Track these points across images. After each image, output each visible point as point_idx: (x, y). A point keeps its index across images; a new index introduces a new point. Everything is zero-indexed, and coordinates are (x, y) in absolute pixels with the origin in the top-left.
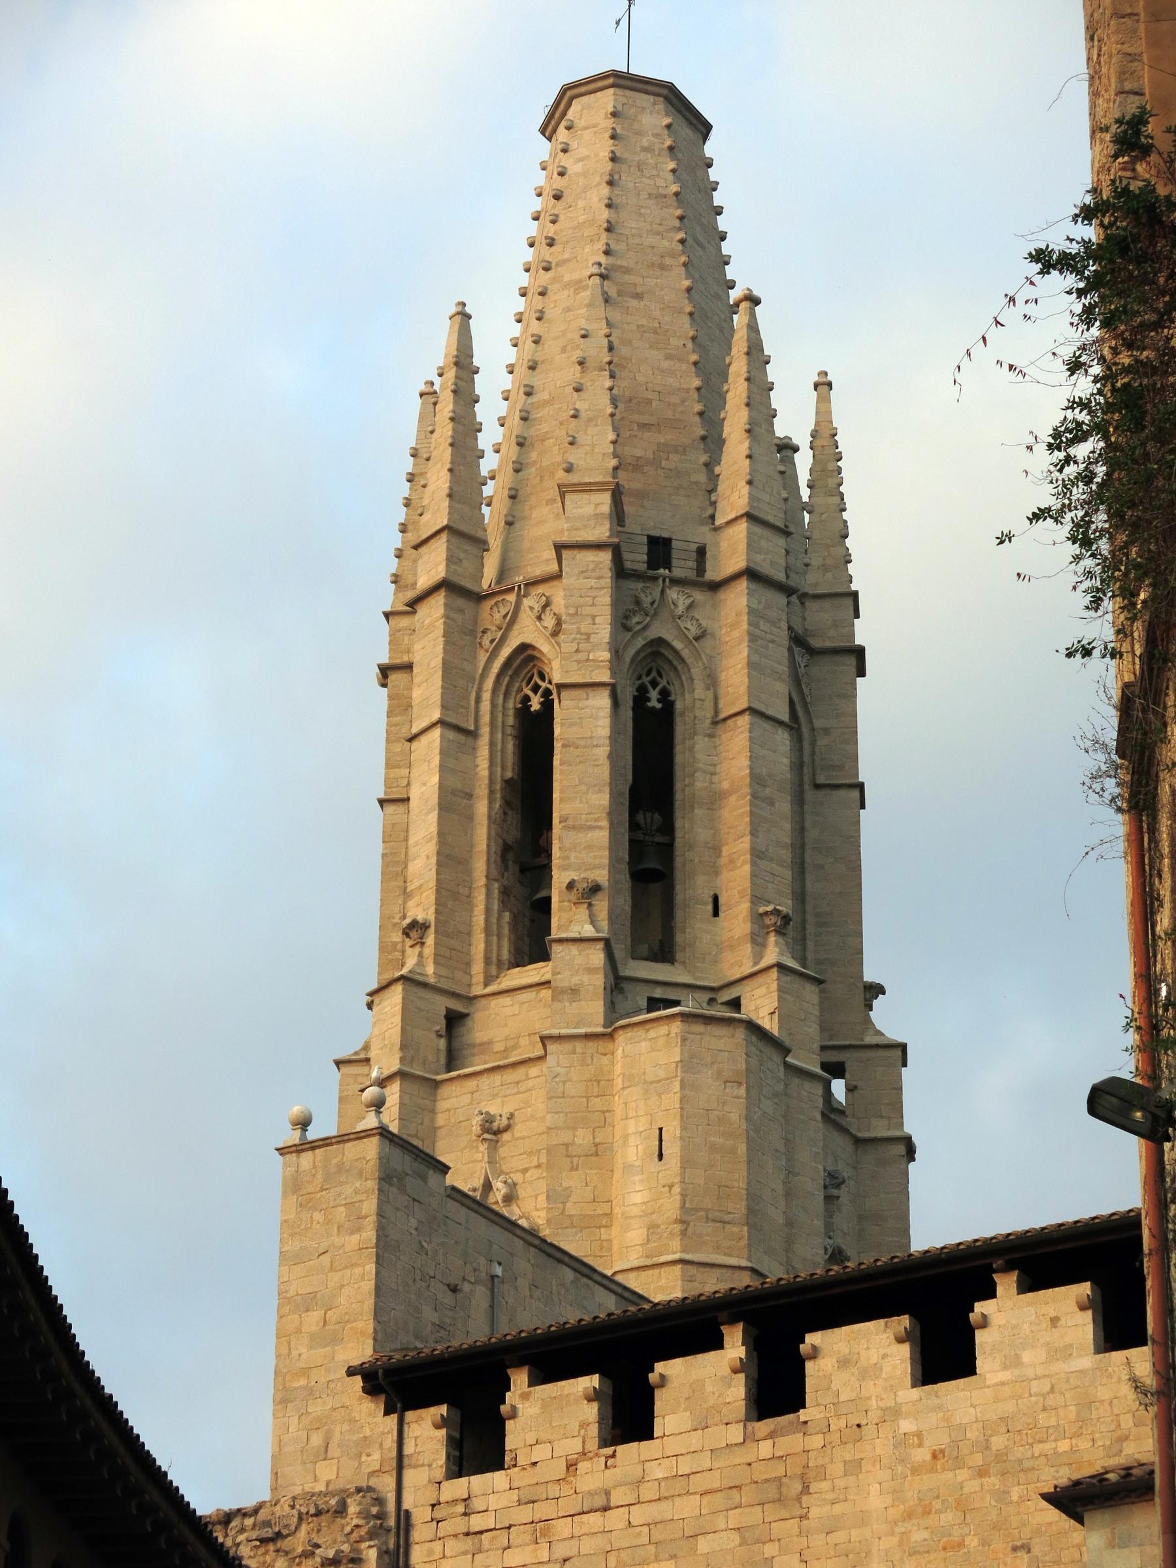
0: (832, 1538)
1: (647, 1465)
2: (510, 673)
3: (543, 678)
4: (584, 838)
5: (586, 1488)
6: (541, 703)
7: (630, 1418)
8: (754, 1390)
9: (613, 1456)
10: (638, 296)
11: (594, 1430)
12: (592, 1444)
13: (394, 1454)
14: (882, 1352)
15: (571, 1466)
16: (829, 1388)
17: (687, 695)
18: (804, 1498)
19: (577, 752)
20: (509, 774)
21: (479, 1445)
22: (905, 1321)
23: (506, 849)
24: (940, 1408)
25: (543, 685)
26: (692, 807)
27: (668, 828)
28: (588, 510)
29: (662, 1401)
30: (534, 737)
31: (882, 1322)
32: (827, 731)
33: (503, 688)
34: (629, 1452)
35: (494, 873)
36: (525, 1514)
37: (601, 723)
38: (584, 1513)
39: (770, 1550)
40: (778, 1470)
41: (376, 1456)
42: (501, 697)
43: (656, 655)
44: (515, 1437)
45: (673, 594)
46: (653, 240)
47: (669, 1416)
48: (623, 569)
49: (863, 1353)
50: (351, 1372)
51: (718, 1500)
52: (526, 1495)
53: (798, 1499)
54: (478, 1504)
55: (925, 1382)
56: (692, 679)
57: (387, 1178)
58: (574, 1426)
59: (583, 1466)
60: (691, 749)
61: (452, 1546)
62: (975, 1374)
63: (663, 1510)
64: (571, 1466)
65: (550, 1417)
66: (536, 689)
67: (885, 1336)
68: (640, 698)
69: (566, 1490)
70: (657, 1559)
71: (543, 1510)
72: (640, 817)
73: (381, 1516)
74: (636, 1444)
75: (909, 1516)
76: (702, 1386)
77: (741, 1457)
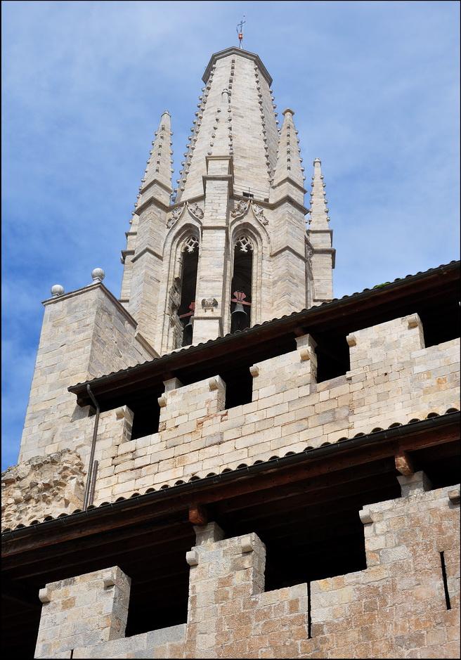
4: (210, 285)
10: (242, 117)
11: (215, 403)
12: (213, 411)
14: (400, 334)
17: (260, 247)
18: (350, 418)
19: (210, 252)
20: (177, 276)
22: (415, 317)
23: (173, 307)
24: (442, 356)
26: (261, 287)
27: (249, 299)
28: (219, 166)
29: (256, 383)
30: (190, 262)
31: (400, 319)
32: (318, 280)
35: (167, 312)
36: (171, 453)
37: (221, 242)
38: (206, 447)
40: (334, 405)
41: (82, 437)
43: (245, 231)
44: (164, 415)
45: (254, 207)
46: (249, 101)
47: (260, 388)
48: (233, 194)
49: (388, 337)
50: (71, 389)
51: (293, 427)
52: (171, 443)
53: (347, 418)
54: (139, 453)
55: (427, 346)
56: (262, 240)
57: (104, 309)
58: (203, 404)
60: (261, 266)
61: (122, 477)
68: (238, 247)
69: (195, 436)
72: (236, 294)
73: (81, 466)
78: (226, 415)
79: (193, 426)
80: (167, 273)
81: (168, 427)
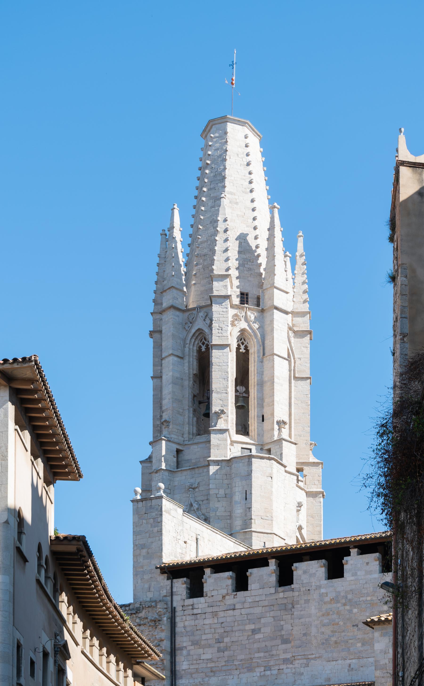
0: (301, 621)
1: (246, 598)
2: (195, 338)
3: (205, 340)
5: (228, 603)
6: (205, 349)
7: (241, 584)
8: (278, 578)
9: (236, 595)
11: (230, 587)
12: (230, 591)
13: (170, 591)
14: (316, 570)
15: (224, 597)
16: (300, 579)
18: (293, 609)
20: (195, 372)
21: (196, 590)
25: (206, 342)
31: (316, 561)
33: (192, 343)
34: (241, 594)
39: (282, 623)
40: (285, 601)
41: (165, 591)
42: (192, 346)
44: (206, 588)
47: (253, 585)
49: (311, 570)
51: (267, 608)
54: (196, 606)
55: (329, 579)
59: (227, 597)
61: (188, 618)
62: (343, 577)
63: (251, 611)
64: (224, 597)
65: (217, 584)
66: (203, 344)
67: (317, 565)
69: (222, 604)
70: (249, 624)
71: (215, 609)
74: (243, 592)
75: (323, 615)
76: (263, 578)
77: (274, 597)
78: (236, 595)
79: (220, 598)
80: (187, 371)
81: (208, 595)
